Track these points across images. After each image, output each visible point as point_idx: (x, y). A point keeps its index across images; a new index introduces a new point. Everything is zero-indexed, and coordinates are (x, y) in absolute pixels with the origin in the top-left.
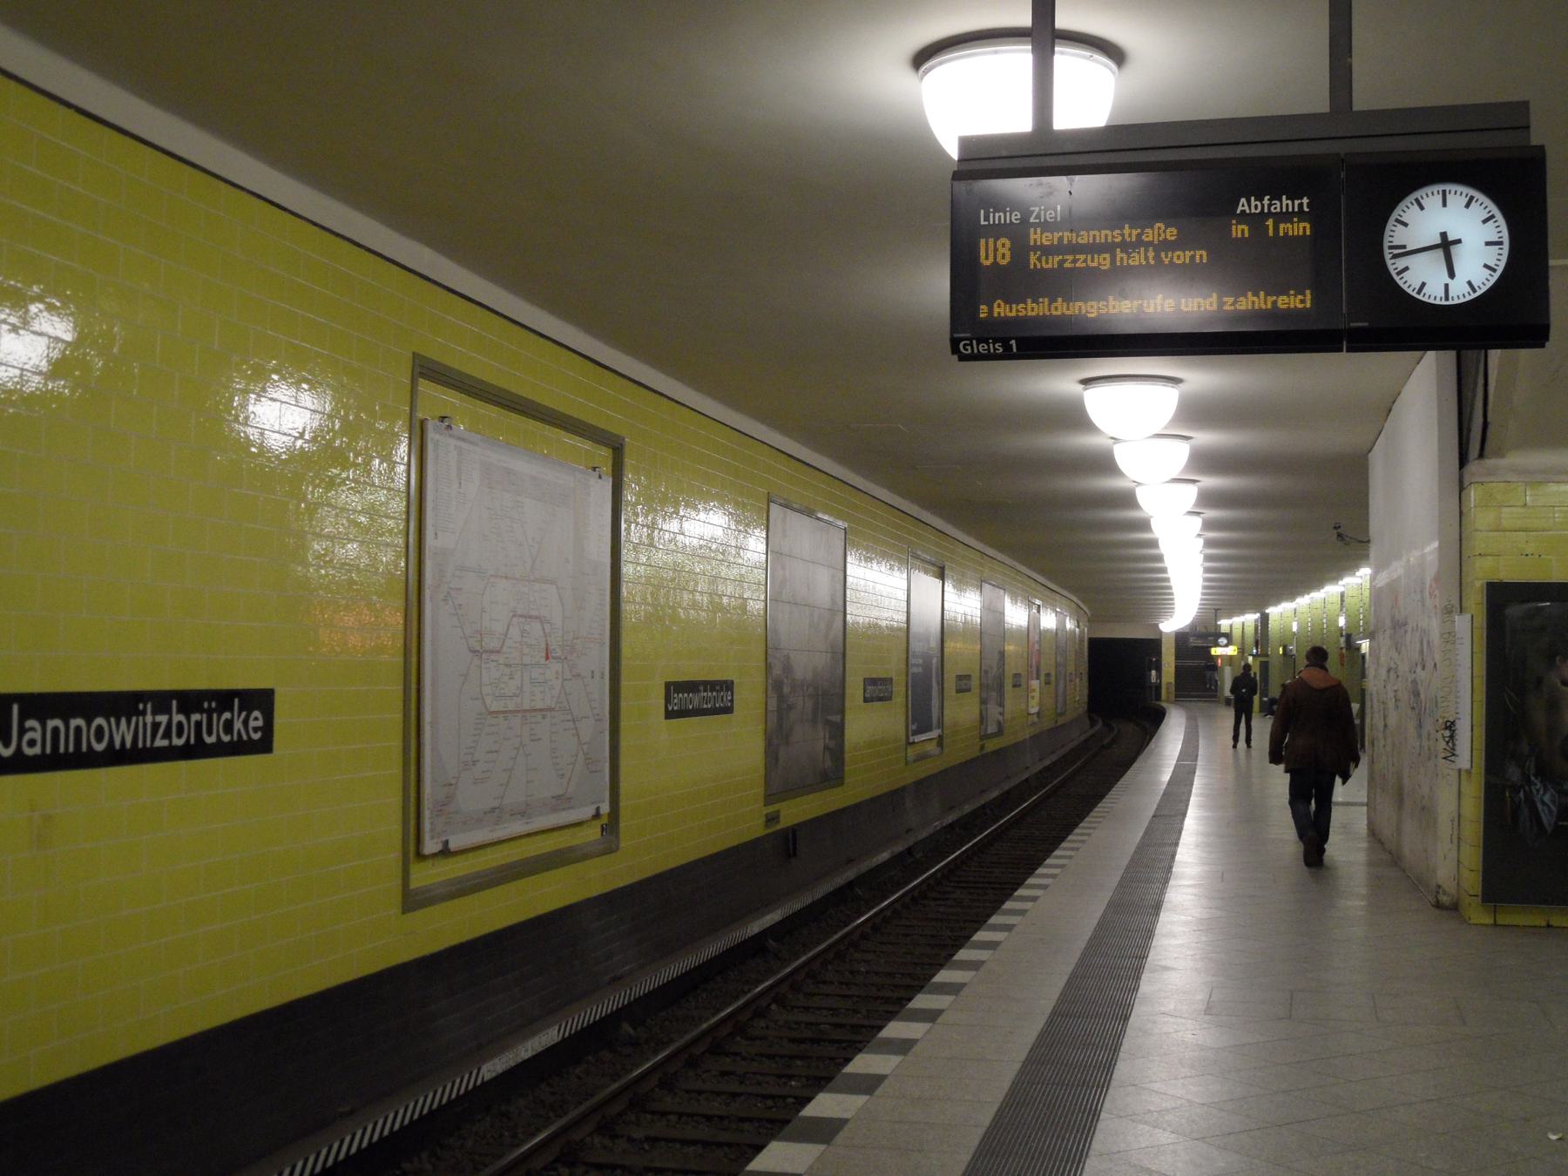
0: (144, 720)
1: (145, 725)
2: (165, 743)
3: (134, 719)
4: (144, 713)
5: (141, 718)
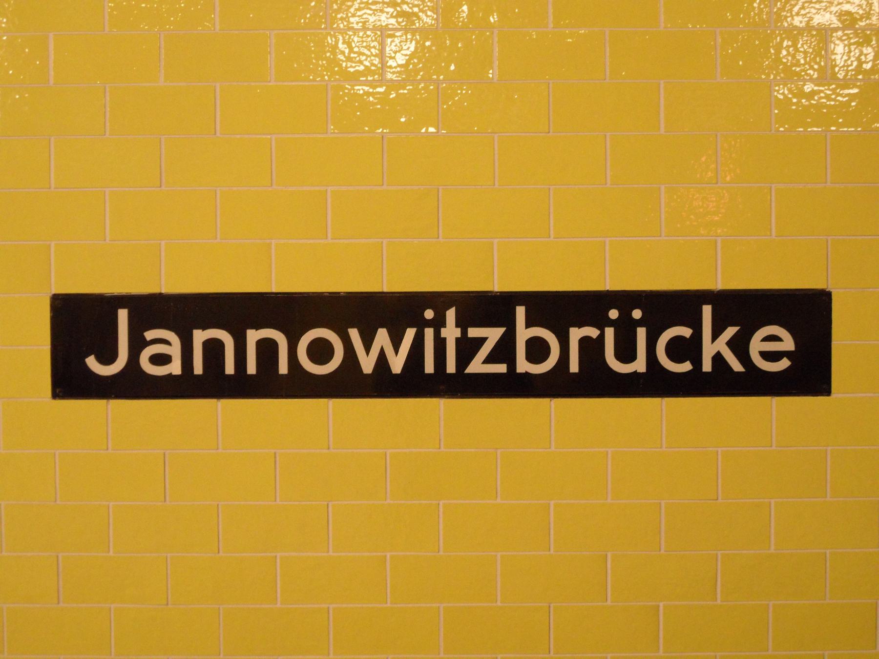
0: (437, 334)
1: (440, 344)
2: (502, 368)
3: (410, 334)
4: (439, 323)
5: (429, 333)
